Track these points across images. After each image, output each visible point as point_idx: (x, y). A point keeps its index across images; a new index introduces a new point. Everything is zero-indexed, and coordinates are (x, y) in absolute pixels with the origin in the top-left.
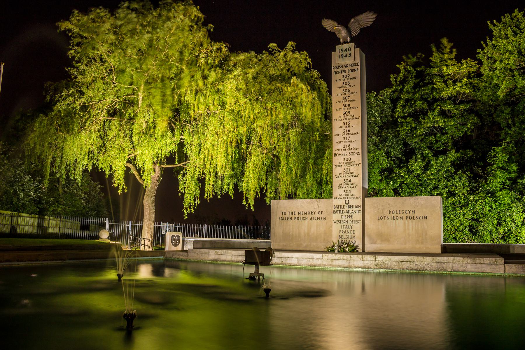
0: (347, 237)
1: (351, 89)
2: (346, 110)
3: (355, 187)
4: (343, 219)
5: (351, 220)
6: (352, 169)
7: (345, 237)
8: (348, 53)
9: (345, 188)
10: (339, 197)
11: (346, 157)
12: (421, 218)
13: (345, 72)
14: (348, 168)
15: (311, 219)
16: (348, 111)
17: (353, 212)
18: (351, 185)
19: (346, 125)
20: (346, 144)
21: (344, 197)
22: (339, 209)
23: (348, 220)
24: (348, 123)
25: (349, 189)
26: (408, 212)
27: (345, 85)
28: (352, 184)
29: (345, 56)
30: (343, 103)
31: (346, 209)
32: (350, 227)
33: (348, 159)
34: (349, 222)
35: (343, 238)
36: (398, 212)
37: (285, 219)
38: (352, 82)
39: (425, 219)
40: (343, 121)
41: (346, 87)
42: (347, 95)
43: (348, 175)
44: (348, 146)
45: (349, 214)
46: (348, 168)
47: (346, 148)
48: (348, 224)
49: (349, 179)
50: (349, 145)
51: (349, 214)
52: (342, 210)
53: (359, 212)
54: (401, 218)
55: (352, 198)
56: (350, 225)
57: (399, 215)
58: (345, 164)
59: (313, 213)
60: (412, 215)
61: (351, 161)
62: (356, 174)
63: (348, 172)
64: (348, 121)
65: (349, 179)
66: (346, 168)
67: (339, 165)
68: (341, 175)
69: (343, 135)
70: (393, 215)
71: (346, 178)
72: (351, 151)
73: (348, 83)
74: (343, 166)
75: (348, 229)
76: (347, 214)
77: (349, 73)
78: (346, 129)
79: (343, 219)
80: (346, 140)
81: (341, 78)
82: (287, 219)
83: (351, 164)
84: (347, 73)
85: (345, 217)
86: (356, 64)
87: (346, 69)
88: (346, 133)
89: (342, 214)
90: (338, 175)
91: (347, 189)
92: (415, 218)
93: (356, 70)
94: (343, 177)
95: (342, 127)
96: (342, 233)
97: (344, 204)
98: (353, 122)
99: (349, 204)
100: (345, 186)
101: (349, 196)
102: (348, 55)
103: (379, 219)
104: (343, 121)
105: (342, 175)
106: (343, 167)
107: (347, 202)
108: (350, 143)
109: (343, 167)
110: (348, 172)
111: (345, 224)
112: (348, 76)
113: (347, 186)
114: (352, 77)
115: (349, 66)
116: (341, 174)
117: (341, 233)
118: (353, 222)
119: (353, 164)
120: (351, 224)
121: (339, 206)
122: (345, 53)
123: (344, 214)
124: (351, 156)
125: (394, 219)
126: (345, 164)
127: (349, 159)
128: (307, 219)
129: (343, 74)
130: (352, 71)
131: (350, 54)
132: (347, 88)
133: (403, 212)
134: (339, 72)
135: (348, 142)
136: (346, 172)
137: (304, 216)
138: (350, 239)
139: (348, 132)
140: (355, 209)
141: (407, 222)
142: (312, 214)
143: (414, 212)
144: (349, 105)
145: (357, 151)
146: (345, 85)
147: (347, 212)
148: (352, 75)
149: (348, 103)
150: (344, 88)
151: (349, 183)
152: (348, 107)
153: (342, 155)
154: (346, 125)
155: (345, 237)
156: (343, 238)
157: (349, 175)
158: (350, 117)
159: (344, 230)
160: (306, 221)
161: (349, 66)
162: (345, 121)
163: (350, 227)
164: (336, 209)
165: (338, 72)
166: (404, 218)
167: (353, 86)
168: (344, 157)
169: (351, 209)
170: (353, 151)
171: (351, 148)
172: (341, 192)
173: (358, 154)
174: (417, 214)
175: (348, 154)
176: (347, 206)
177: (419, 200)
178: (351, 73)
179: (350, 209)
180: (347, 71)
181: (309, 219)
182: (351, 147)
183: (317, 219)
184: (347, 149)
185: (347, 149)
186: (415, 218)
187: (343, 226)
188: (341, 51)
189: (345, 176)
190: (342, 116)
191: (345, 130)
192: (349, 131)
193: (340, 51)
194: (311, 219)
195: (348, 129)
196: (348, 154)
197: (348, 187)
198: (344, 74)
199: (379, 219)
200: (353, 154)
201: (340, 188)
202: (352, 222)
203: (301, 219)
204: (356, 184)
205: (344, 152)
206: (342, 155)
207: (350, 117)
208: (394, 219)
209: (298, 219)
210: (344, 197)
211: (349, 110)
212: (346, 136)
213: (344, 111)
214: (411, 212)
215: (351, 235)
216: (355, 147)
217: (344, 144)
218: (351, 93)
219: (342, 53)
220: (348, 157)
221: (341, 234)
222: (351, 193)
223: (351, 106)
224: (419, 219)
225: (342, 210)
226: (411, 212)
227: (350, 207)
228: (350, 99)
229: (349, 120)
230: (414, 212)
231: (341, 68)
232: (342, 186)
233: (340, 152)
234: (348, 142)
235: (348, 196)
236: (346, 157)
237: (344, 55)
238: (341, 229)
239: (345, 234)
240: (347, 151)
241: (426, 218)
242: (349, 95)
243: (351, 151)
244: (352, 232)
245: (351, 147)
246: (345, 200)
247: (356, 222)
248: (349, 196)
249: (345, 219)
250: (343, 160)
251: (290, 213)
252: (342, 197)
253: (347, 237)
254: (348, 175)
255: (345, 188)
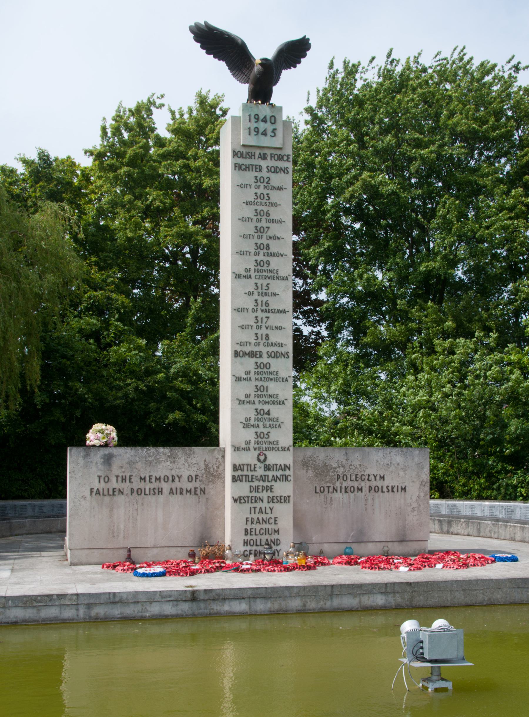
0: (262, 531)
1: (272, 209)
2: (261, 257)
3: (280, 426)
4: (254, 494)
5: (271, 495)
6: (274, 388)
7: (258, 532)
8: (269, 127)
9: (258, 426)
10: (244, 446)
11: (259, 361)
12: (395, 489)
13: (260, 170)
14: (265, 384)
15: (171, 492)
16: (265, 259)
17: (275, 479)
18: (271, 423)
19: (260, 290)
20: (259, 332)
21: (256, 446)
22: (245, 473)
23: (265, 495)
24: (265, 287)
25: (265, 431)
26: (372, 477)
27: (259, 200)
28: (272, 420)
29: (262, 134)
30: (256, 240)
31: (260, 472)
32: (268, 511)
33: (265, 366)
34: (265, 500)
35: (253, 533)
36: (354, 477)
37: (106, 492)
38: (275, 196)
39: (403, 491)
40: (253, 281)
41: (261, 204)
42: (264, 224)
43: (264, 399)
44: (264, 337)
45: (266, 484)
46: (265, 384)
47: (260, 340)
48: (265, 505)
49: (266, 407)
50: (267, 336)
51: (266, 484)
52: (250, 474)
53: (286, 479)
54: (360, 490)
55: (273, 449)
56: (268, 505)
57: (356, 484)
58: (257, 376)
59: (177, 479)
60: (379, 483)
61: (271, 370)
62: (281, 398)
63: (265, 393)
64: (265, 282)
65: (266, 407)
66: (259, 384)
67: (245, 376)
68: (248, 400)
69: (254, 311)
70: (345, 484)
71: (260, 407)
72: (271, 349)
73: (266, 197)
74: (253, 379)
75: (264, 516)
76: (261, 483)
77: (268, 175)
78: (260, 299)
79: (254, 494)
80: (259, 324)
81: (252, 181)
82: (111, 493)
83: (271, 377)
84: (265, 174)
85: (257, 489)
86: (285, 158)
87: (264, 164)
88: (259, 307)
89: (251, 484)
90: (243, 398)
91: (261, 429)
92: (385, 490)
93: (285, 171)
94: (254, 403)
95: (250, 294)
96: (252, 523)
97: (256, 462)
98: (276, 286)
99: (267, 463)
100: (256, 423)
101: (267, 446)
102: (269, 133)
103: (318, 490)
104: (253, 281)
105: (252, 398)
106: (254, 383)
107: (262, 458)
108: (268, 331)
109: (254, 383)
110: (265, 393)
111: (259, 505)
112: (266, 180)
113: (261, 424)
114: (276, 185)
115: (269, 158)
116: (248, 396)
117: (249, 523)
118: (275, 500)
119: (276, 378)
120: (271, 505)
121: (245, 467)
122: (262, 126)
123: (256, 483)
124: (271, 361)
125: (346, 492)
126: (257, 376)
127: (267, 366)
128: (160, 491)
129: (256, 174)
130: (276, 170)
131: (274, 131)
132: (265, 209)
133: (363, 477)
134: (247, 168)
135: (264, 328)
136: (259, 393)
137: (155, 485)
138: (267, 537)
139: (264, 307)
140: (279, 473)
141: (370, 499)
142: (173, 481)
143: (382, 478)
144: (268, 245)
145: (283, 350)
146: (259, 200)
147: (263, 478)
148: (276, 179)
149: (264, 241)
150: (256, 207)
151: (266, 416)
152: (265, 251)
153: (252, 354)
154: (260, 290)
155: (258, 532)
156: (253, 533)
157: (267, 399)
158: (270, 275)
159: (255, 517)
160: (161, 498)
161: (269, 158)
162: (260, 282)
163: (268, 511)
164: (239, 473)
165: (243, 167)
166: (366, 490)
167: (275, 205)
168: (254, 360)
169: (270, 474)
170: (275, 349)
171: (270, 341)
172: (249, 435)
173: (285, 355)
174: (388, 482)
175: (265, 355)
176: (262, 465)
177: (392, 454)
178: (273, 176)
179: (267, 473)
180: (265, 169)
181: (166, 490)
182: (273, 339)
183: (184, 492)
184: (262, 343)
185: (262, 343)
186: (385, 490)
187: (253, 510)
188: (253, 120)
189: (257, 402)
190: (253, 268)
191: (259, 302)
192: (267, 304)
193: (252, 118)
194: (171, 492)
195: (265, 299)
196: (265, 355)
197: (265, 426)
198: (259, 175)
199: (318, 490)
200: (276, 355)
201: (246, 426)
202: (271, 500)
203: (147, 492)
204: (280, 420)
205: (255, 349)
206: (252, 354)
207: (270, 275)
208: (346, 492)
209: (139, 492)
210: (256, 446)
211: (268, 258)
212: (259, 314)
213: (256, 258)
214: (378, 477)
215: (273, 526)
216: (279, 341)
217: (257, 331)
218: (273, 221)
219: (255, 125)
220: (265, 360)
221: (249, 527)
222: (271, 439)
223: (273, 249)
224: (393, 491)
225: (250, 474)
226: (378, 477)
227: (267, 468)
228: (270, 233)
229: (268, 281)
230: (382, 478)
231: (251, 158)
232: (252, 422)
233: (247, 349)
234: (264, 328)
235: (264, 446)
236: (259, 361)
237: (261, 130)
238: (250, 516)
239: (258, 527)
240: (264, 350)
241: (404, 489)
242: (268, 225)
243: (271, 349)
244: (272, 521)
245: (273, 339)
246: (257, 452)
247: (284, 500)
248: (267, 446)
249: (257, 495)
250: (254, 366)
251: (120, 479)
252: (252, 445)
253: (262, 531)
254: (264, 399)
255: (258, 426)
